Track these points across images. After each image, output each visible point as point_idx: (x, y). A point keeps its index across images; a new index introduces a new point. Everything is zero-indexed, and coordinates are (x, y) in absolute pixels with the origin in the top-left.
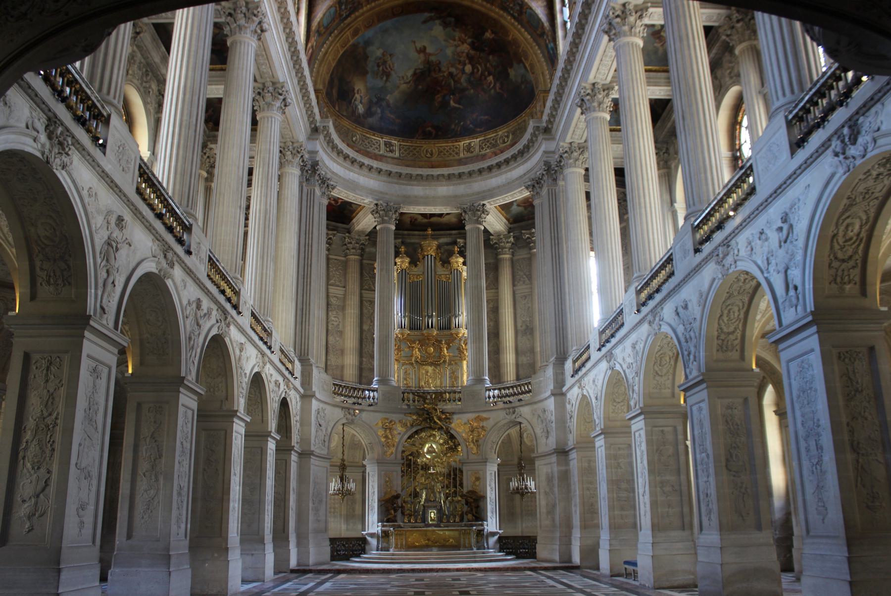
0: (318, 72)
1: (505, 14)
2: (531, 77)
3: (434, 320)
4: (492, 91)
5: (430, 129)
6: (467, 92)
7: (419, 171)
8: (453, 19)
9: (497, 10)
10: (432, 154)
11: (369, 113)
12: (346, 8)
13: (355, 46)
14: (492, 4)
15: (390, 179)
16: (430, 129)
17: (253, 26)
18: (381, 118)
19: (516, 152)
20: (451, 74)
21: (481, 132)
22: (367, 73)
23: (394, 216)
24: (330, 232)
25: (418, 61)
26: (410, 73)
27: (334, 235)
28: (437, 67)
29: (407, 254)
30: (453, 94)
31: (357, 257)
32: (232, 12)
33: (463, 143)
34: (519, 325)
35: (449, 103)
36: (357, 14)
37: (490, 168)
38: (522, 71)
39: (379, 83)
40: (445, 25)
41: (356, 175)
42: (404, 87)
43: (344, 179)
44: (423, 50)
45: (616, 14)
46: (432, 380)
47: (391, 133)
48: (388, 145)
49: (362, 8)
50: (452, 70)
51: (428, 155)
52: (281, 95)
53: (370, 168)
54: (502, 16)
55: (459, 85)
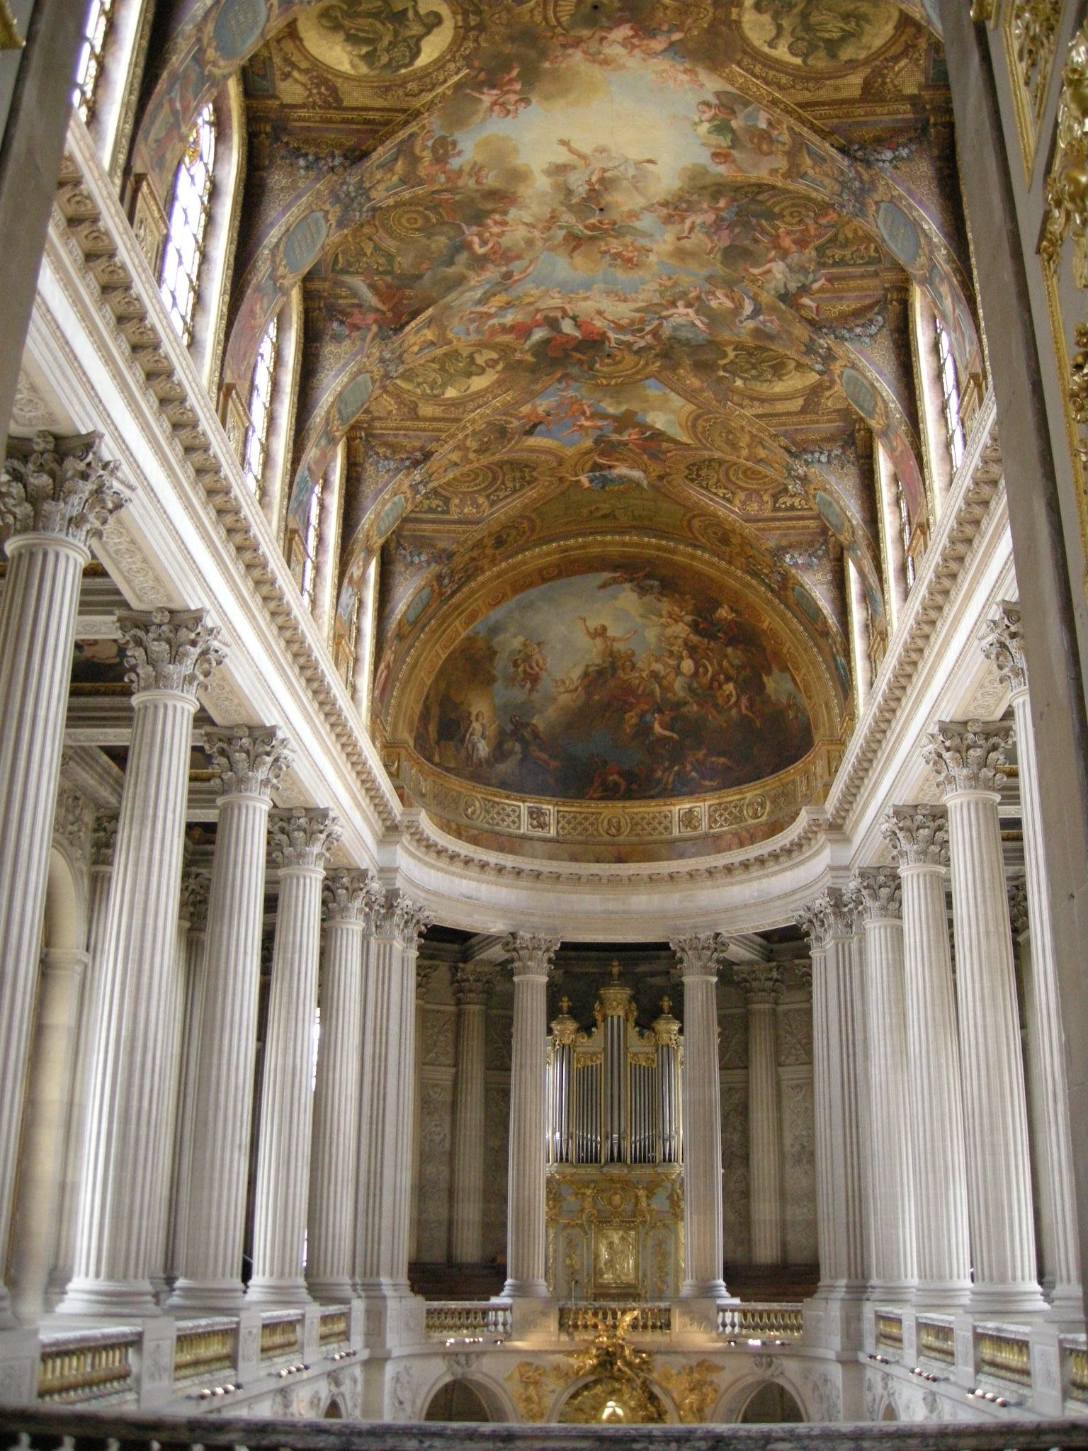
0: (399, 705)
1: (754, 582)
2: (805, 702)
3: (626, 1144)
4: (734, 712)
5: (615, 777)
6: (685, 710)
7: (595, 868)
8: (657, 583)
9: (739, 573)
10: (618, 830)
11: (499, 753)
12: (451, 581)
13: (471, 639)
14: (730, 563)
15: (539, 885)
16: (615, 777)
17: (262, 773)
18: (523, 759)
19: (777, 847)
20: (654, 675)
21: (714, 789)
22: (493, 679)
23: (546, 957)
24: (427, 963)
25: (592, 652)
26: (576, 673)
27: (436, 968)
28: (629, 661)
29: (574, 1014)
30: (660, 711)
31: (477, 1007)
32: (225, 746)
33: (679, 808)
34: (788, 1142)
35: (652, 728)
36: (473, 584)
37: (729, 869)
38: (790, 686)
39: (518, 695)
40: (642, 591)
41: (474, 884)
42: (564, 699)
43: (450, 898)
44: (601, 632)
45: (948, 744)
46: (617, 1256)
47: (542, 791)
48: (535, 814)
49: (483, 572)
50: (657, 667)
51: (613, 831)
52: (321, 832)
53: (500, 870)
54: (749, 586)
55: (669, 695)
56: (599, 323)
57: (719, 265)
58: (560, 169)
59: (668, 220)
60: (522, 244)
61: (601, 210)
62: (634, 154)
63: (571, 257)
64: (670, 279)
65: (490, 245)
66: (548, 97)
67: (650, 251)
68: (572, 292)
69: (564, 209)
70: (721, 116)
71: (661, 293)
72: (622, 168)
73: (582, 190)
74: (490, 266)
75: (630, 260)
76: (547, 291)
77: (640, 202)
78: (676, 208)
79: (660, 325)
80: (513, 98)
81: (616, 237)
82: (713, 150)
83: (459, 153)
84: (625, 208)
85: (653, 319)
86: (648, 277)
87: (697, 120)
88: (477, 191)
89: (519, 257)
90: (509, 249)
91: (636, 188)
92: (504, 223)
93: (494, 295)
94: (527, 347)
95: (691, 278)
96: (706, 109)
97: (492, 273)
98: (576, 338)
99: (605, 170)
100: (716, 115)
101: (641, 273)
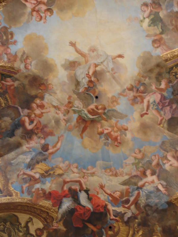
56: (102, 197)
57: (166, 131)
58: (72, 65)
59: (134, 101)
60: (53, 121)
61: (97, 97)
62: (112, 52)
63: (82, 138)
64: (140, 151)
65: (35, 123)
66: (62, 9)
67: (126, 130)
68: (84, 168)
69: (75, 96)
70: (154, 10)
71: (136, 164)
72: (105, 63)
73: (84, 82)
74: (35, 138)
75: (116, 139)
76: (69, 165)
77: (118, 89)
78: (138, 91)
79: (139, 194)
80: (43, 7)
81: (107, 121)
82: (154, 38)
83: (15, 42)
84: (110, 95)
85: (133, 190)
86: (127, 153)
87: (142, 18)
88: (26, 77)
89: (51, 134)
90: (46, 126)
91: (114, 78)
92: (42, 106)
93: (38, 163)
94: (60, 216)
95: (152, 151)
96: (146, 9)
97: (36, 143)
98: (89, 210)
99: (96, 66)
100: (151, 11)
101: (123, 149)
